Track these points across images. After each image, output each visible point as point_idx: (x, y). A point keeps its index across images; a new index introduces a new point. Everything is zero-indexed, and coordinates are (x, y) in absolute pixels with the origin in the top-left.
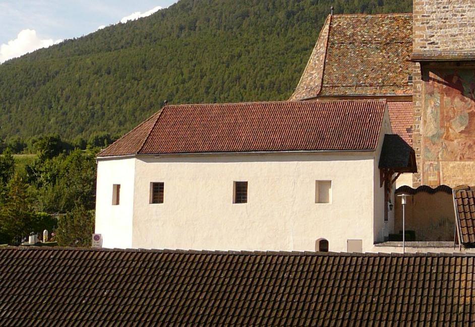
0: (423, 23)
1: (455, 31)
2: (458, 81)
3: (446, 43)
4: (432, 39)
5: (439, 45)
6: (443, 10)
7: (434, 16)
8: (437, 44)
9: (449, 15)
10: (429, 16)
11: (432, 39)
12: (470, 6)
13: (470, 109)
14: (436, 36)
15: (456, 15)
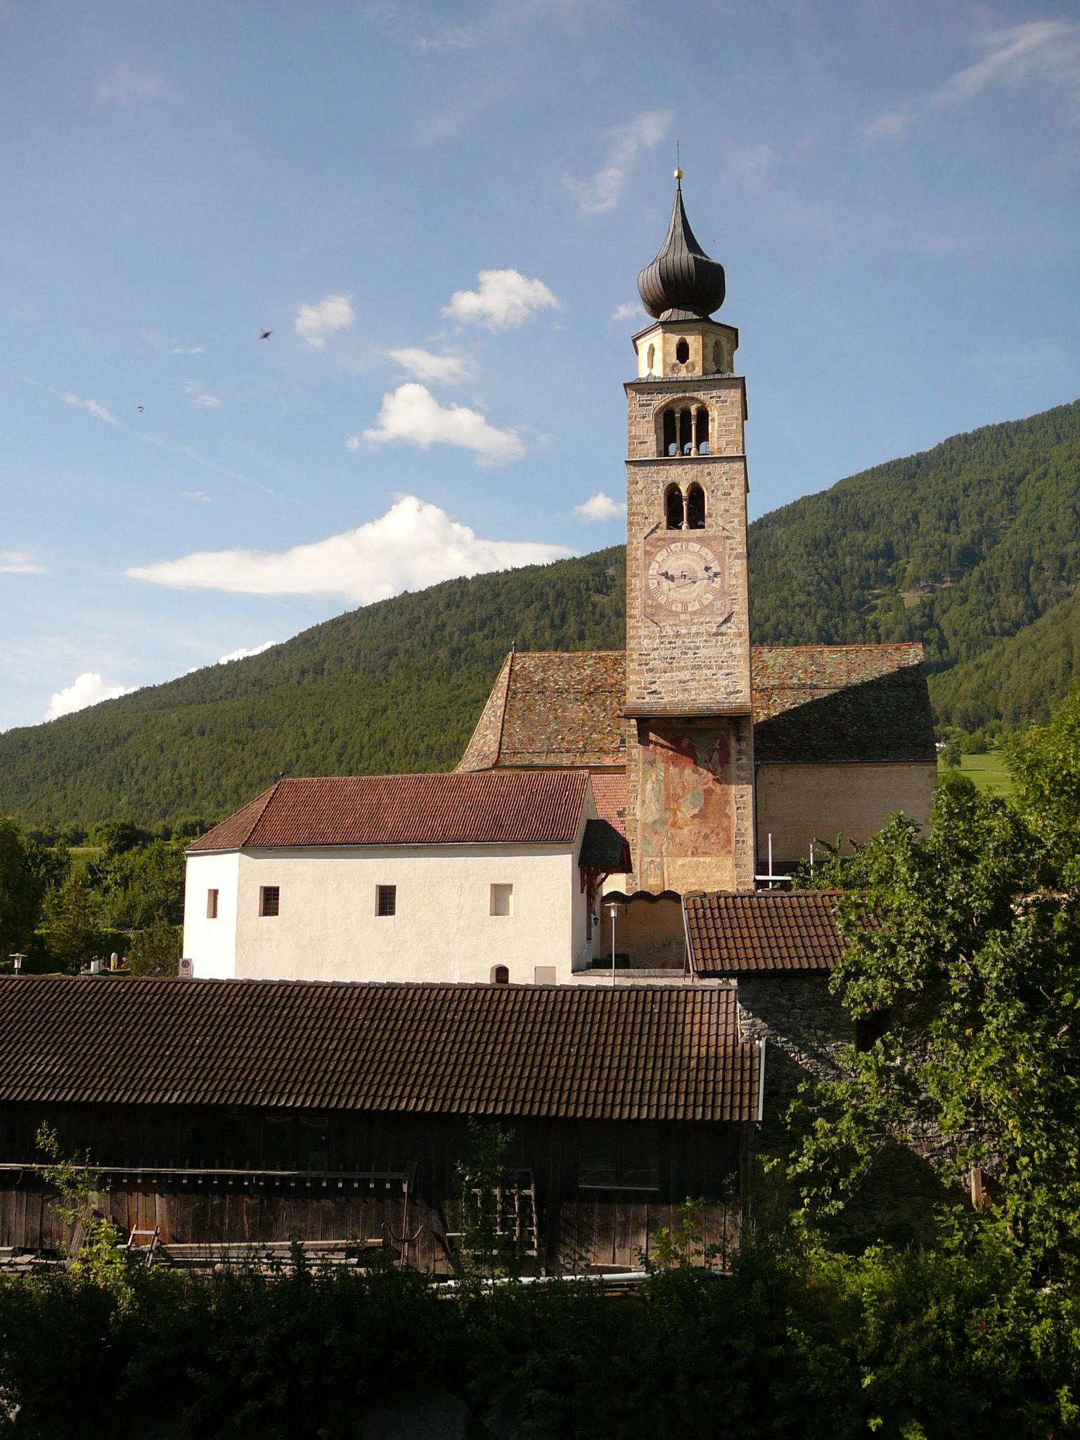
0: (640, 665)
1: (685, 675)
2: (690, 746)
3: (672, 692)
4: (654, 687)
5: (663, 695)
6: (668, 646)
7: (656, 653)
8: (660, 693)
9: (676, 653)
10: (649, 655)
11: (653, 686)
12: (706, 641)
13: (706, 784)
14: (658, 682)
15: (686, 653)
